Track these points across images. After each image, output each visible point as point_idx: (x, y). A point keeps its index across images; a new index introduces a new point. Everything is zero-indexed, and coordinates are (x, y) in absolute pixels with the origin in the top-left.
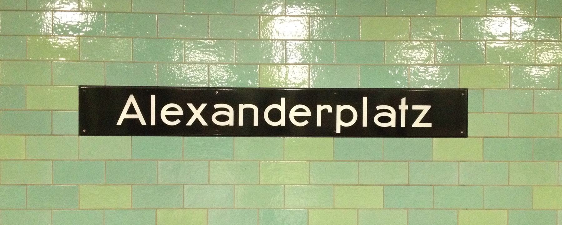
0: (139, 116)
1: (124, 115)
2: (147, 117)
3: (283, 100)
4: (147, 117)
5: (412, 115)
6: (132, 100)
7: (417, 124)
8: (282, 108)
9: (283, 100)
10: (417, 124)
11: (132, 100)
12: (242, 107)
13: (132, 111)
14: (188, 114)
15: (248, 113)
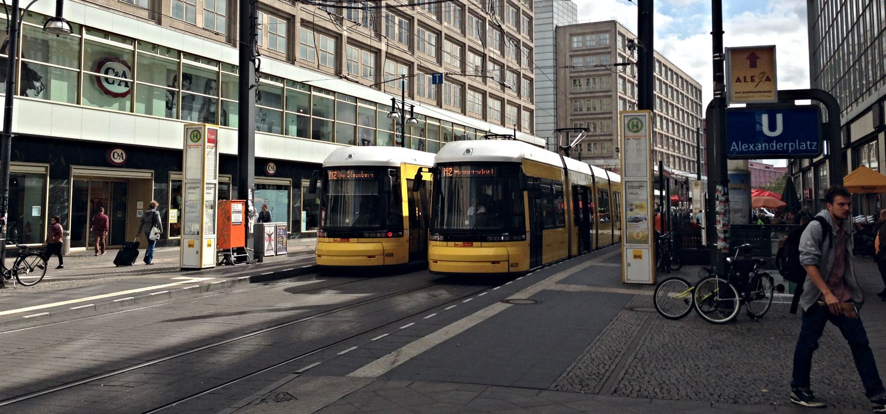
0: (736, 148)
1: (732, 148)
2: (738, 147)
3: (775, 141)
4: (738, 147)
5: (811, 145)
6: (734, 143)
7: (813, 148)
8: (774, 145)
9: (775, 141)
10: (813, 148)
11: (734, 143)
12: (763, 145)
13: (734, 146)
14: (749, 147)
15: (765, 145)
